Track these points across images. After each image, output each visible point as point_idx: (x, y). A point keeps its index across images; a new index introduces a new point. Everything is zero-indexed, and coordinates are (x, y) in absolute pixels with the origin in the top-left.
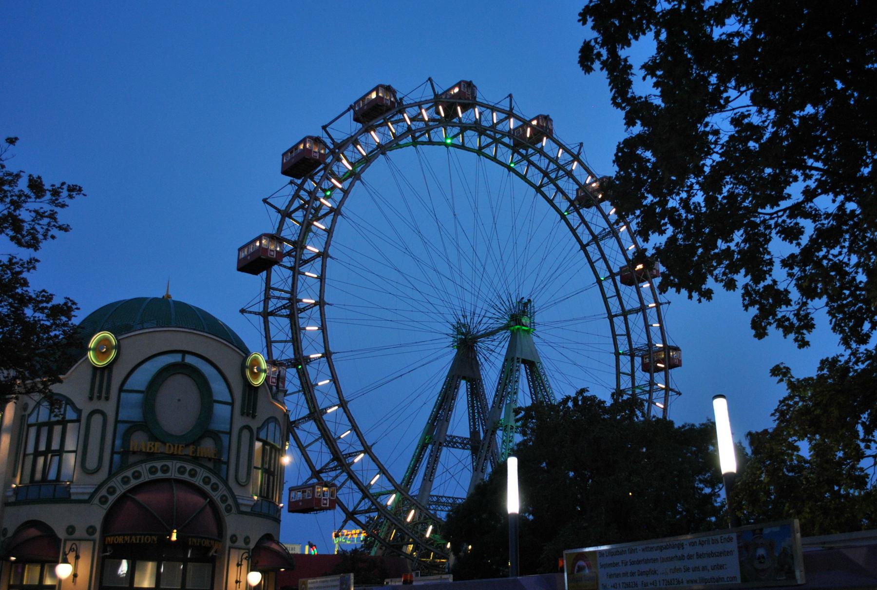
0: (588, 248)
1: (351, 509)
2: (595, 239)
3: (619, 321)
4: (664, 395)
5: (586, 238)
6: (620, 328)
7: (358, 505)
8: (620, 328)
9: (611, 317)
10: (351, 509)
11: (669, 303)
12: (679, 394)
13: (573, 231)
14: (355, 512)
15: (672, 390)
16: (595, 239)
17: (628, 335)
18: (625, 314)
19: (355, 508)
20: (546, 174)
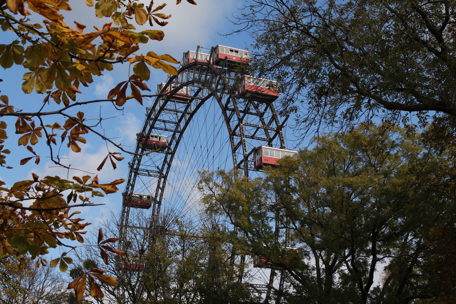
9: (165, 177)
11: (129, 163)
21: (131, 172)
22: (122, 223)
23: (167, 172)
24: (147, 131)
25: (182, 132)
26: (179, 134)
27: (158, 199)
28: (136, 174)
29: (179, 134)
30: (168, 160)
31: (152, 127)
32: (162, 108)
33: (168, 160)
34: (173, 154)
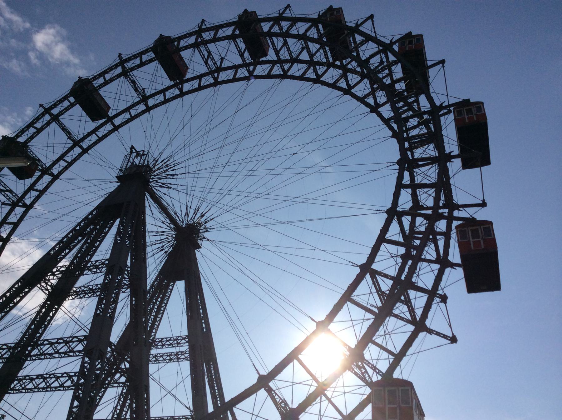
0: (85, 147)
1: (411, 328)
2: (77, 143)
3: (151, 102)
4: (207, 33)
5: (77, 150)
6: (161, 98)
7: (402, 319)
8: (161, 98)
9: (148, 109)
10: (411, 328)
11: (120, 55)
12: (203, 21)
13: (70, 164)
14: (413, 321)
15: (200, 27)
16: (77, 143)
17: (163, 91)
18: (144, 99)
19: (408, 321)
20: (14, 205)
21: (116, 66)
22: (51, 108)
23: (156, 106)
24: (183, 43)
25: (217, 83)
26: (212, 81)
27: (117, 122)
28: (125, 73)
29: (212, 81)
30: (169, 94)
31: (196, 45)
32: (232, 37)
33: (169, 94)
34: (182, 94)
